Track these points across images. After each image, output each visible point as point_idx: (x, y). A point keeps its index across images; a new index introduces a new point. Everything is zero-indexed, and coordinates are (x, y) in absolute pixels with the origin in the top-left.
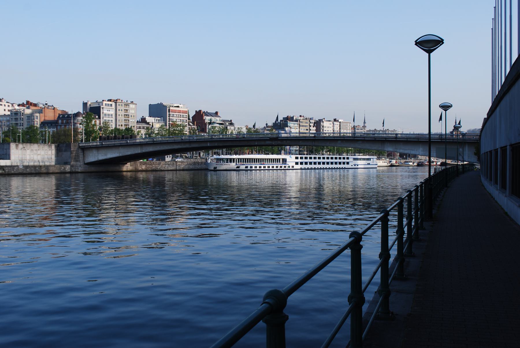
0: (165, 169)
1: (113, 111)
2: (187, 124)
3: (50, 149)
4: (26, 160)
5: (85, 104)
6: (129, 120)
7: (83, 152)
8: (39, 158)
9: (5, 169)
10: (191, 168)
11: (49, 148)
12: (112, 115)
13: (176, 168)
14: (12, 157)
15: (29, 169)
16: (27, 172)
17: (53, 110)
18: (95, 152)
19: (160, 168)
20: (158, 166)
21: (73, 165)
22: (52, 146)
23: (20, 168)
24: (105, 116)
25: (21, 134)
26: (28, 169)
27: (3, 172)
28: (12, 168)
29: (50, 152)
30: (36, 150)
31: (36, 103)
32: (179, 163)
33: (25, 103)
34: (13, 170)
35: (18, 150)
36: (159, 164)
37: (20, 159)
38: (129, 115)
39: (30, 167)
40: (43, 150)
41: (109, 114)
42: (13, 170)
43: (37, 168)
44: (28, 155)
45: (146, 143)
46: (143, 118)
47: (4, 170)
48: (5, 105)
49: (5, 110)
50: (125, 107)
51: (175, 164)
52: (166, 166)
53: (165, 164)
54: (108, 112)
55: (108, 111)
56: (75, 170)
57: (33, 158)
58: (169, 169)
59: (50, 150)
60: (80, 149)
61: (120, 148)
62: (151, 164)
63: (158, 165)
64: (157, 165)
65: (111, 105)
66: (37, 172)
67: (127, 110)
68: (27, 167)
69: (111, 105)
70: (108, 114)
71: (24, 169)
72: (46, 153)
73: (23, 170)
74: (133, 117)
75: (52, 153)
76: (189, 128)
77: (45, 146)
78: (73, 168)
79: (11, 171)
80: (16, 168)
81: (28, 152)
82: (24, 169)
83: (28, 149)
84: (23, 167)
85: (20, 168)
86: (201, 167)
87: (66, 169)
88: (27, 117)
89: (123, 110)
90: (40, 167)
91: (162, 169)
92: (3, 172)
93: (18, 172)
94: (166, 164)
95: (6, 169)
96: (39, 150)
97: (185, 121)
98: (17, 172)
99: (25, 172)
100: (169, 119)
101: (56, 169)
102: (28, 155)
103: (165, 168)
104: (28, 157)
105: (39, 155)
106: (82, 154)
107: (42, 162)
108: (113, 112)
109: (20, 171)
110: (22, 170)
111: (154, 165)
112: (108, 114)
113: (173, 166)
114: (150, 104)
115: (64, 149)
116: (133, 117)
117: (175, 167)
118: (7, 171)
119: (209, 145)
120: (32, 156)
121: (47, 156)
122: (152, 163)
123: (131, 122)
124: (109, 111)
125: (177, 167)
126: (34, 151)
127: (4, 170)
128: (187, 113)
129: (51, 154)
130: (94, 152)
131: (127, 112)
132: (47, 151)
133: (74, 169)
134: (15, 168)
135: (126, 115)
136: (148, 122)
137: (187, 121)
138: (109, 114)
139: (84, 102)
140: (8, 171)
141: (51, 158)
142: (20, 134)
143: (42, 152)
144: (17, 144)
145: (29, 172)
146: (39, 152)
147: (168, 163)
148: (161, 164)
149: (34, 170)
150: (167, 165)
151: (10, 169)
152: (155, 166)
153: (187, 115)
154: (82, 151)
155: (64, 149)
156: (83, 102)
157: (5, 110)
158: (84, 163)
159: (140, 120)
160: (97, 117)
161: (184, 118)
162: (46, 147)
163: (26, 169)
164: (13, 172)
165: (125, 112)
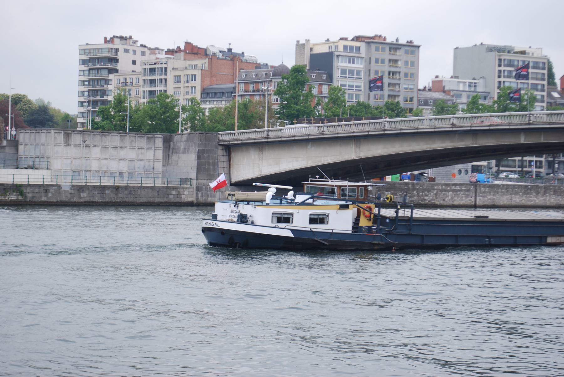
0: (445, 204)
1: (361, 64)
2: (545, 94)
3: (151, 145)
4: (90, 171)
5: (300, 47)
6: (401, 85)
7: (229, 155)
8: (123, 167)
9: (25, 191)
10: (518, 201)
11: (148, 143)
12: (358, 73)
13: (475, 201)
14: (57, 164)
15: (87, 192)
16: (82, 200)
17: (232, 62)
18: (253, 155)
19: (432, 199)
20: (426, 195)
21: (202, 187)
22: (156, 140)
23: (64, 191)
24: (341, 74)
25: (128, 113)
27: (20, 198)
28: (42, 189)
29: (150, 155)
30: (115, 148)
31: (205, 47)
32: (483, 189)
33: (182, 48)
34: (46, 196)
35: (69, 147)
36: (428, 190)
37: (74, 168)
38: (400, 72)
39: (88, 189)
40: (132, 148)
41: (353, 71)
42: (46, 196)
44: (95, 159)
45: (367, 133)
46: (437, 79)
47: (21, 193)
48: (135, 52)
49: (134, 62)
50: (390, 54)
51: (473, 191)
52: (448, 196)
53: (445, 190)
54: (351, 65)
55: (350, 62)
56: (204, 198)
57: (108, 168)
58: (456, 203)
59: (150, 148)
60: (220, 148)
61: (309, 146)
62: (409, 188)
63: (426, 192)
64: (423, 192)
65: (358, 49)
66: (107, 200)
67: (396, 61)
69: (358, 49)
70: (349, 71)
71: (73, 191)
72: (141, 157)
73: (71, 194)
74: (409, 78)
75: (154, 154)
76: (551, 103)
77: (139, 139)
78: (200, 195)
79: (41, 197)
80: (52, 190)
81: (96, 152)
82: (73, 191)
83: (95, 146)
84: (71, 189)
85: (63, 189)
86: (544, 200)
87: (183, 196)
88: (175, 76)
89: (387, 62)
90: (114, 190)
91: (438, 203)
92: (20, 198)
93: (59, 199)
94: (448, 191)
95: (28, 191)
96: (121, 148)
97: (539, 87)
98: (54, 200)
99: (75, 199)
100: (500, 82)
101: (156, 194)
102: (95, 159)
103: (444, 200)
104: (95, 165)
105: (121, 159)
106: (225, 159)
107: (131, 175)
108: (362, 66)
109: (64, 198)
110: (69, 195)
111: (415, 192)
112: (349, 71)
113: (467, 196)
114: (457, 48)
115: (182, 146)
116: (409, 78)
117: (473, 199)
118: (29, 196)
119: (522, 140)
120: (105, 162)
121: (142, 163)
122: (410, 186)
123: (405, 88)
124: (353, 63)
125: (478, 199)
126: (111, 151)
127: (21, 193)
128: (543, 69)
129: (152, 158)
130: (253, 157)
131: (397, 67)
132: (143, 151)
133: (202, 196)
134: (51, 190)
135: (394, 73)
136: (446, 88)
137: (546, 87)
138: (353, 71)
139: (301, 43)
140: (33, 197)
141: (154, 168)
142: (127, 112)
143: (132, 154)
144: (68, 133)
145: (87, 199)
146: (122, 153)
147: (453, 188)
148: (434, 190)
149: (99, 195)
150: (451, 193)
151: (37, 190)
152: (418, 194)
153: (545, 72)
154: (225, 154)
155: (182, 147)
156: (296, 43)
157: (134, 62)
158: (230, 182)
159: (431, 85)
160: (324, 77)
161: (537, 79)
162: (141, 142)
164: (44, 199)
165: (391, 66)
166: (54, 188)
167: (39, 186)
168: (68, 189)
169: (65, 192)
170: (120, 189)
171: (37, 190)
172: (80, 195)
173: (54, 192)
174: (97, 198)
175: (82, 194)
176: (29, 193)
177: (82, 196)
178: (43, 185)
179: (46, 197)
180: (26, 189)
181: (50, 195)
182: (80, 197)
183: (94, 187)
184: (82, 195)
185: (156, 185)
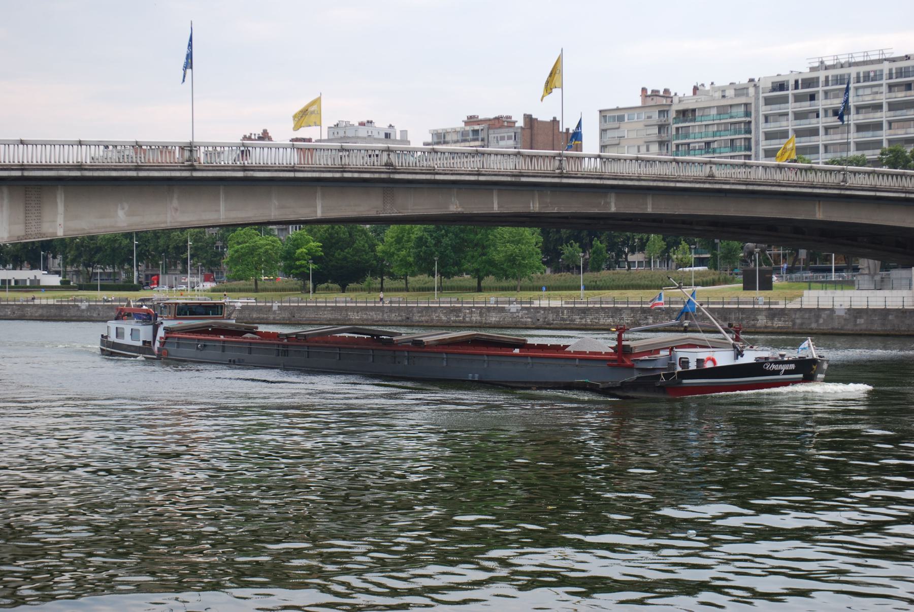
15: (865, 317)
23: (838, 316)
26: (861, 317)
42: (817, 321)
43: (890, 317)
68: (858, 313)
71: (847, 316)
73: (845, 320)
79: (810, 324)
80: (824, 315)
82: (847, 316)
84: (846, 314)
85: (837, 313)
99: (849, 327)
110: (843, 322)
118: (798, 321)
134: (823, 315)
140: (802, 324)
145: (864, 327)
163: (856, 318)
164: (814, 326)
166: (827, 312)
167: (810, 310)
168: (842, 313)
169: (839, 317)
170: (908, 314)
171: (807, 316)
172: (855, 321)
173: (826, 318)
174: (876, 326)
175: (858, 320)
176: (798, 318)
177: (858, 322)
178: (867, 309)
179: (816, 324)
180: (796, 314)
181: (821, 321)
182: (856, 325)
183: (874, 310)
184: (859, 321)
185: (870, 307)
